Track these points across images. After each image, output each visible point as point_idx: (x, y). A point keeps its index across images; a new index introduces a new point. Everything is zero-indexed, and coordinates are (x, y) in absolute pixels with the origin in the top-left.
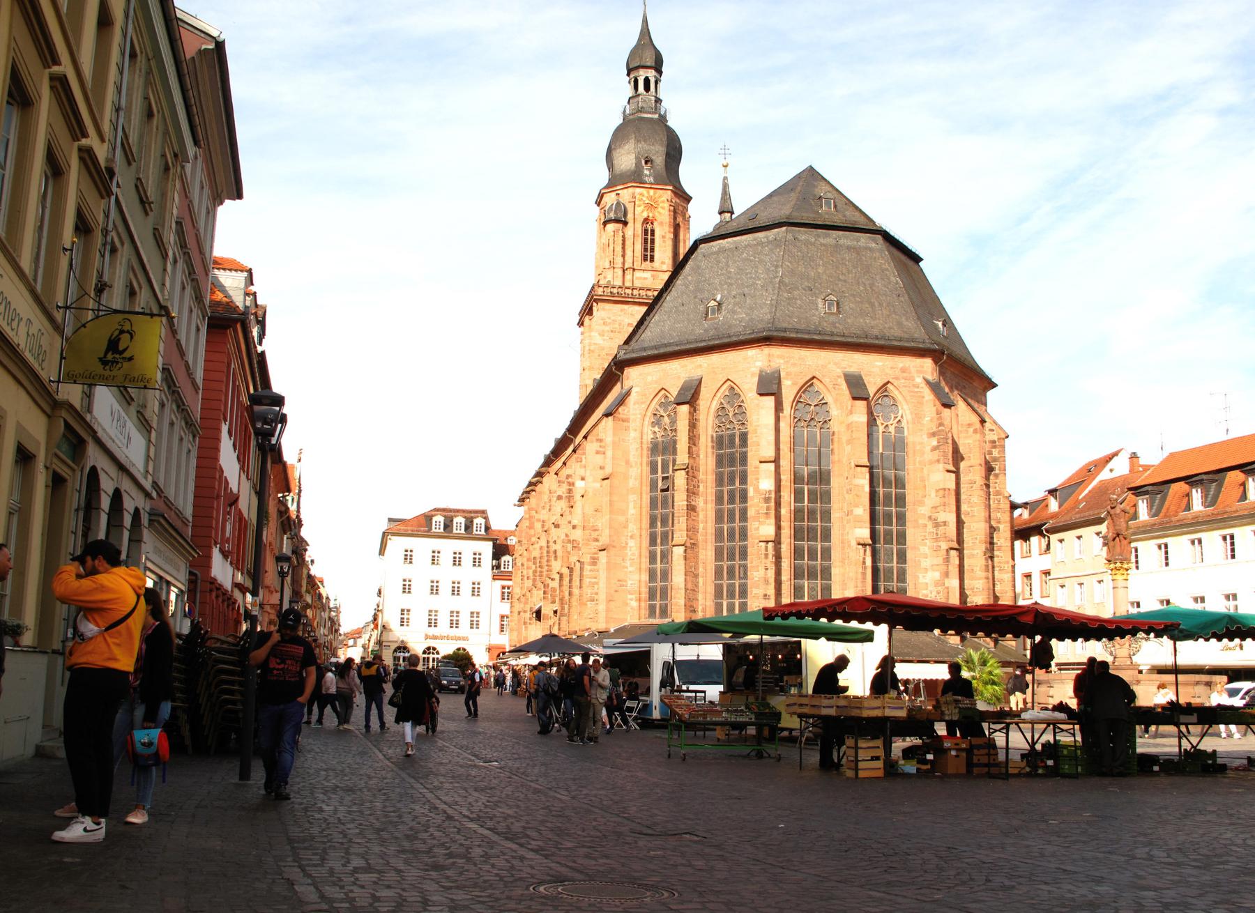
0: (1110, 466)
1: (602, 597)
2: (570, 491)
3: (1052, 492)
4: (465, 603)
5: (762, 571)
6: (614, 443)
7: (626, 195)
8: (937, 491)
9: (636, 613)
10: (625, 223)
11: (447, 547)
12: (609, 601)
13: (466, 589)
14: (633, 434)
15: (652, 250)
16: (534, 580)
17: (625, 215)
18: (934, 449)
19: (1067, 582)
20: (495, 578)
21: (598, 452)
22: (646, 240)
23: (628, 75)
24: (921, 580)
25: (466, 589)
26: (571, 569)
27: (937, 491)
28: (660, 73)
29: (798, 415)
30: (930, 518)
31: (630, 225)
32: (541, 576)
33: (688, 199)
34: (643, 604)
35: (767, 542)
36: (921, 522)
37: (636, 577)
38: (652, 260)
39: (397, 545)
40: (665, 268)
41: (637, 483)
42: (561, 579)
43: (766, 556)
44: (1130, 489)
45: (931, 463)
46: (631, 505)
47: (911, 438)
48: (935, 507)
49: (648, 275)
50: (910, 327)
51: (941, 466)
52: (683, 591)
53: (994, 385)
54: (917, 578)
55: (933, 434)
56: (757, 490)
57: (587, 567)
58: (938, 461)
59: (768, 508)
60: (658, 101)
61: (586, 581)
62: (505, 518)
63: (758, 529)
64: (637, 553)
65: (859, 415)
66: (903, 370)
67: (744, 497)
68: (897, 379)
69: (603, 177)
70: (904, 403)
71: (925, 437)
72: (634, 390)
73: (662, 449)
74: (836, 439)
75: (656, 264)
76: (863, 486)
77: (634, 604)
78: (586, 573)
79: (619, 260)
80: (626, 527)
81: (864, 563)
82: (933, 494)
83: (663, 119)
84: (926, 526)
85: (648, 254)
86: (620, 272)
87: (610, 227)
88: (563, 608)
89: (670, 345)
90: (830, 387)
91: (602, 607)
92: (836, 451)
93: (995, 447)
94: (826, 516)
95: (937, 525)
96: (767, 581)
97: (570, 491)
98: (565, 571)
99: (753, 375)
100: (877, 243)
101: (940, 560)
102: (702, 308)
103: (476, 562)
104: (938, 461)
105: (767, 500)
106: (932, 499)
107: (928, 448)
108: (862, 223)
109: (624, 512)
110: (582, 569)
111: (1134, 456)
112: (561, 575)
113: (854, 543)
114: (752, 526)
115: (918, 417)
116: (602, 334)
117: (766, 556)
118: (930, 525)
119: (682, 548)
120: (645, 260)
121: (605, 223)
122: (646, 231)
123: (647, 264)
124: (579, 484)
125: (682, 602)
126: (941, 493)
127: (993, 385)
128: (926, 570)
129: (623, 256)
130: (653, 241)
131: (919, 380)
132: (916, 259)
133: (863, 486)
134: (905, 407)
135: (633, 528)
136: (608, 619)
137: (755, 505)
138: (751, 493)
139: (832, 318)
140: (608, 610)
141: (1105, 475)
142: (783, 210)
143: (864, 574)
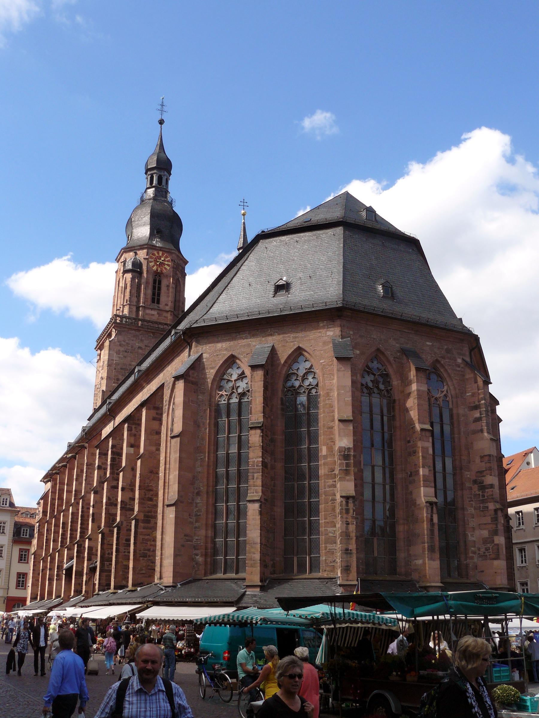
8: (482, 457)
15: (159, 295)
21: (154, 419)
22: (154, 288)
23: (146, 173)
24: (470, 538)
27: (482, 457)
28: (170, 174)
30: (475, 482)
33: (186, 262)
34: (209, 560)
36: (468, 485)
37: (203, 532)
38: (158, 302)
40: (167, 308)
48: (481, 472)
49: (155, 313)
54: (465, 535)
57: (141, 525)
59: (348, 465)
60: (167, 192)
61: (140, 537)
68: (443, 357)
70: (448, 379)
71: (466, 410)
72: (205, 356)
74: (397, 407)
75: (161, 306)
76: (427, 449)
77: (200, 559)
81: (432, 520)
82: (478, 460)
83: (171, 204)
85: (156, 298)
86: (134, 309)
87: (129, 276)
90: (391, 359)
99: (325, 343)
101: (488, 519)
105: (346, 457)
116: (118, 353)
118: (475, 488)
119: (257, 506)
120: (153, 302)
123: (155, 305)
125: (257, 556)
128: (474, 529)
130: (159, 289)
131: (459, 361)
134: (449, 383)
138: (324, 451)
142: (337, 214)
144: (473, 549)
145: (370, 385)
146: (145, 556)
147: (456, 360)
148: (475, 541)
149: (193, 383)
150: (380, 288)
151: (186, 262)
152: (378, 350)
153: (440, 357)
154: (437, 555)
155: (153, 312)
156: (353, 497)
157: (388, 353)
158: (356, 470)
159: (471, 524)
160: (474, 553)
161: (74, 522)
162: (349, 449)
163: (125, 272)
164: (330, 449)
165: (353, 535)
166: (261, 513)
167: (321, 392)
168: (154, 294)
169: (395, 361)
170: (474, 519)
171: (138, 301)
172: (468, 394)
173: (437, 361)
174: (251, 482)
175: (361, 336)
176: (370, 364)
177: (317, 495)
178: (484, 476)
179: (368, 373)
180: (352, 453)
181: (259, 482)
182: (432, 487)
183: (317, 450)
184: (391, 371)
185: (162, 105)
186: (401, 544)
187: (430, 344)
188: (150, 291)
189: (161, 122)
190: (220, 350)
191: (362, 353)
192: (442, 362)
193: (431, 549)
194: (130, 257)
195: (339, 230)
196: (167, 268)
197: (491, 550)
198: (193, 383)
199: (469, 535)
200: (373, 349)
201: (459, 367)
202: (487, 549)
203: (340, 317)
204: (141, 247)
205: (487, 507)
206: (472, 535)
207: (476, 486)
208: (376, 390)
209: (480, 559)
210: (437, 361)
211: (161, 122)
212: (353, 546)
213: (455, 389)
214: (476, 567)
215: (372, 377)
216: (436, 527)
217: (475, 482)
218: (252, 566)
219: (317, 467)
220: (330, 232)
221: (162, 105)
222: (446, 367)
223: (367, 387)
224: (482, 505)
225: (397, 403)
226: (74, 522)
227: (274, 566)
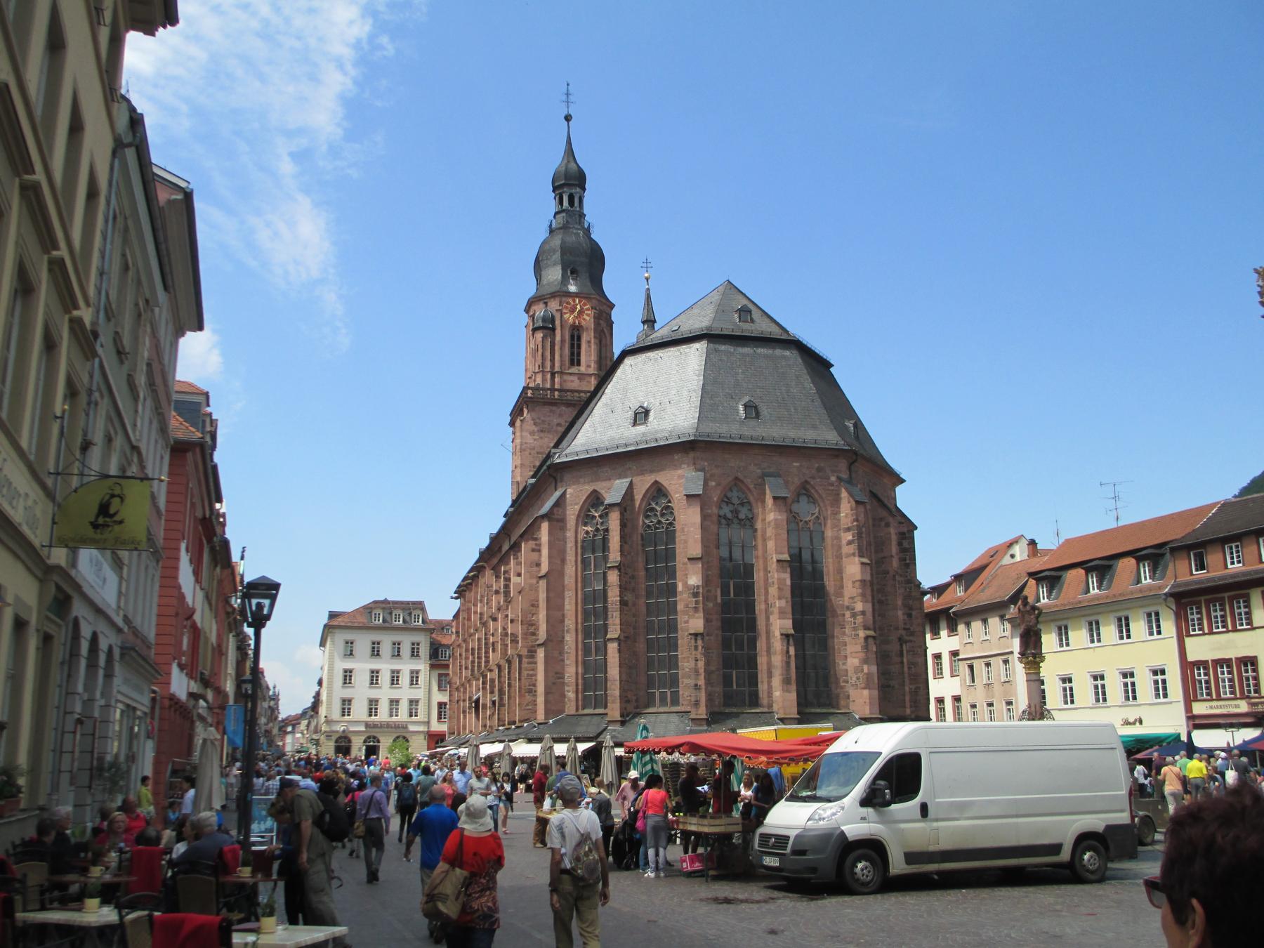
0: (1011, 552)
1: (541, 688)
2: (507, 586)
3: (957, 578)
4: (405, 693)
5: (692, 664)
6: (549, 542)
7: (554, 305)
9: (574, 704)
10: (553, 329)
11: (386, 641)
12: (547, 693)
13: (405, 679)
14: (570, 534)
15: (579, 354)
16: (473, 670)
17: (553, 320)
18: (849, 543)
19: (976, 663)
20: (433, 667)
21: (533, 550)
22: (572, 346)
24: (842, 667)
25: (405, 679)
26: (509, 662)
28: (584, 189)
29: (722, 513)
31: (558, 332)
32: (479, 666)
33: (612, 306)
35: (696, 635)
38: (579, 364)
39: (340, 638)
40: (591, 371)
41: (573, 580)
42: (500, 671)
43: (696, 648)
44: (1031, 575)
45: (848, 556)
46: (567, 602)
48: (852, 598)
51: (857, 559)
52: (618, 683)
53: (903, 481)
55: (848, 529)
56: (685, 584)
57: (525, 660)
58: (854, 554)
59: (697, 603)
60: (582, 215)
61: (525, 673)
62: (442, 608)
63: (687, 622)
64: (573, 647)
66: (819, 470)
67: (671, 590)
68: (813, 478)
69: (531, 289)
73: (595, 546)
75: (583, 369)
77: (571, 695)
78: (524, 665)
79: (548, 364)
80: (563, 621)
81: (788, 652)
82: (850, 585)
83: (587, 232)
85: (575, 360)
86: (549, 376)
87: (539, 335)
88: (501, 699)
89: (602, 449)
90: (751, 486)
91: (541, 700)
92: (760, 547)
93: (905, 538)
94: (750, 607)
95: (854, 615)
96: (696, 671)
97: (507, 586)
98: (503, 663)
101: (859, 648)
102: (631, 414)
103: (415, 653)
104: (854, 554)
105: (695, 595)
107: (844, 542)
108: (776, 332)
109: (561, 608)
110: (520, 663)
111: (1032, 543)
112: (499, 667)
113: (777, 634)
114: (681, 619)
116: (532, 433)
117: (696, 648)
118: (848, 614)
121: (535, 330)
122: (572, 337)
123: (574, 370)
124: (514, 579)
125: (617, 693)
126: (858, 584)
127: (903, 481)
129: (553, 360)
130: (579, 347)
131: (833, 479)
132: (829, 365)
135: (570, 622)
136: (548, 713)
137: (683, 600)
138: (680, 587)
139: (753, 423)
140: (546, 702)
141: (1007, 560)
143: (788, 663)
145: (729, 515)
146: (530, 691)
149: (558, 521)
150: (741, 408)
151: (612, 306)
152: (737, 478)
154: (794, 687)
155: (571, 378)
156: (702, 634)
157: (748, 481)
158: (711, 605)
159: (843, 653)
161: (479, 649)
163: (535, 330)
164: (685, 584)
165: (702, 671)
166: (620, 651)
167: (678, 527)
168: (572, 354)
171: (553, 366)
173: (806, 482)
174: (610, 621)
175: (717, 466)
176: (729, 495)
177: (676, 631)
179: (727, 503)
181: (618, 621)
183: (675, 585)
184: (751, 498)
185: (568, 94)
186: (762, 676)
188: (567, 351)
189: (568, 118)
191: (718, 484)
193: (786, 681)
194: (539, 310)
195: (701, 346)
196: (588, 319)
198: (558, 521)
200: (730, 479)
204: (553, 295)
208: (735, 521)
210: (806, 482)
211: (568, 118)
212: (702, 682)
214: (848, 697)
215: (731, 507)
216: (793, 659)
217: (848, 608)
218: (613, 702)
219: (675, 603)
220: (696, 345)
221: (568, 94)
223: (725, 517)
226: (479, 649)
227: (637, 701)
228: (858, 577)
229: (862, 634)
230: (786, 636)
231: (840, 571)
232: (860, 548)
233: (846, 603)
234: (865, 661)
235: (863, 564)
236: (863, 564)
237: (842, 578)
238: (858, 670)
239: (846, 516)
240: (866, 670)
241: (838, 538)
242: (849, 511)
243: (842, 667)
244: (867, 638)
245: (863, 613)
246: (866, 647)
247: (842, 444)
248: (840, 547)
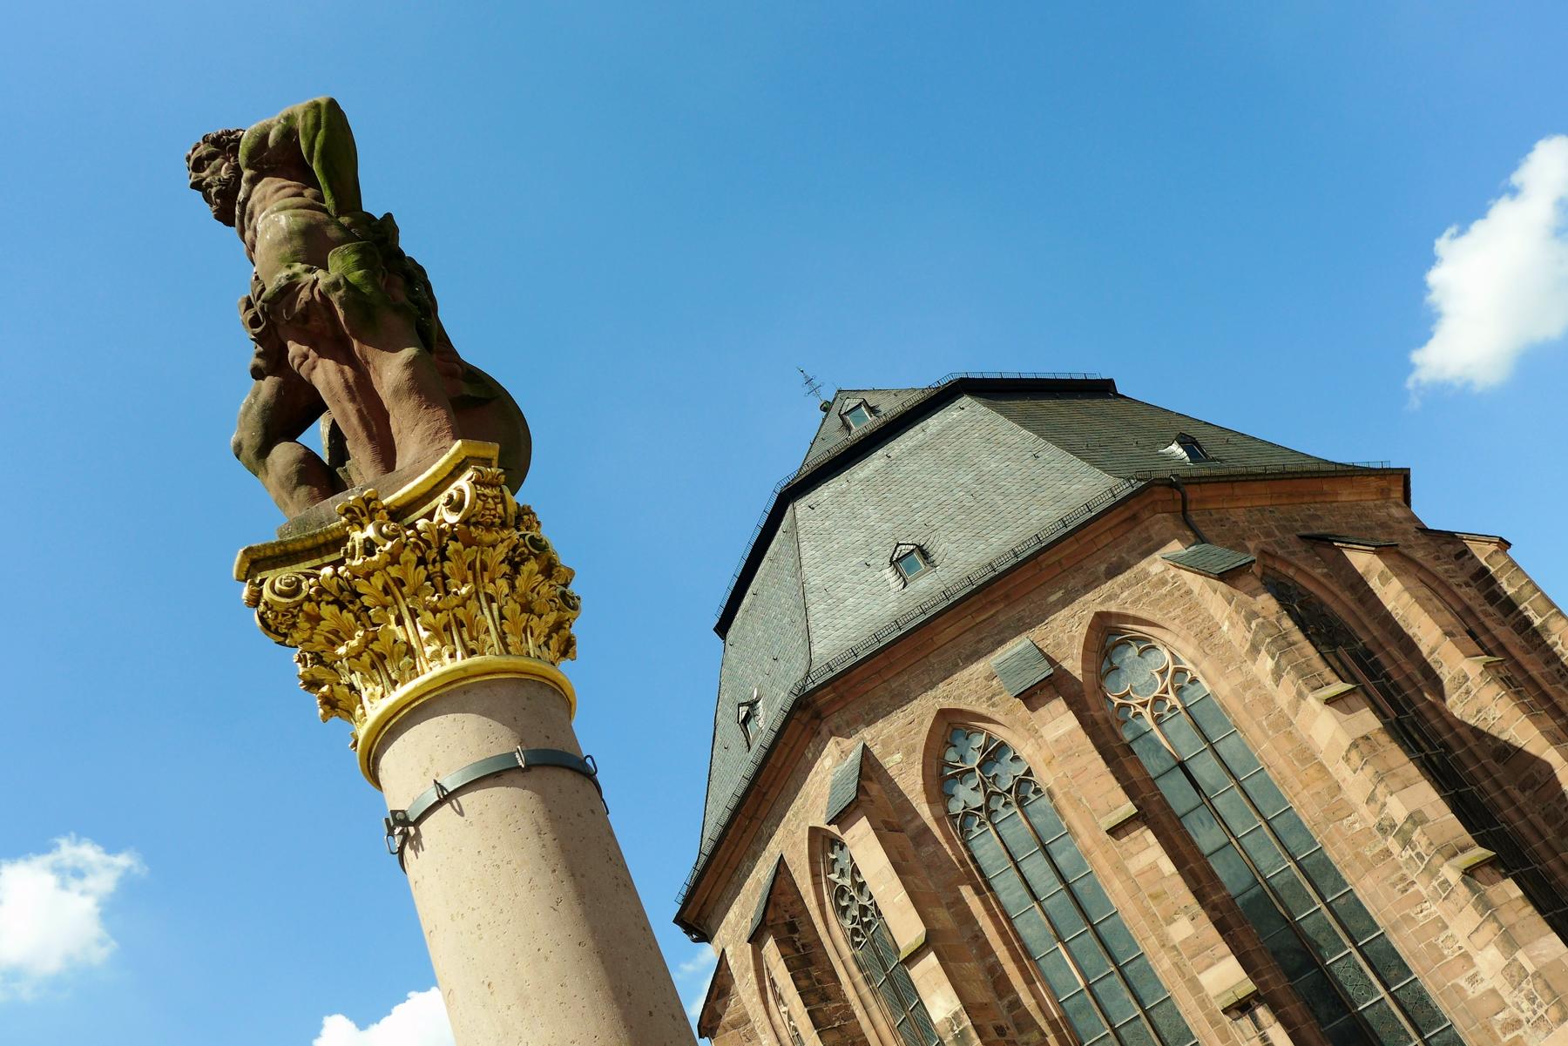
18: (1277, 675)
24: (1473, 992)
27: (1347, 759)
30: (1382, 829)
47: (1216, 683)
48: (1371, 799)
50: (1078, 486)
55: (1255, 649)
58: (1301, 695)
65: (1059, 721)
76: (1154, 867)
84: (1387, 853)
100: (966, 409)
104: (1301, 695)
106: (1355, 782)
107: (1268, 681)
115: (1207, 636)
118: (1393, 844)
126: (1354, 755)
128: (1466, 957)
132: (1104, 388)
133: (1154, 867)
134: (1167, 638)
144: (1501, 1016)
147: (1148, 574)
148: (1494, 991)
153: (1101, 603)
160: (1517, 1024)
162: (956, 1016)
169: (993, 705)
170: (1449, 932)
172: (1225, 628)
178: (1384, 805)
180: (967, 1023)
182: (1223, 957)
187: (1060, 594)
190: (737, 924)
191: (909, 752)
192: (1114, 610)
197: (1539, 999)
199: (1463, 983)
201: (1164, 582)
202: (1532, 1000)
203: (818, 716)
205: (1446, 881)
206: (1473, 980)
207: (1390, 838)
209: (1541, 1034)
213: (1185, 640)
222: (1131, 612)
224: (1435, 883)
225: (1056, 790)
228: (1346, 743)
229: (1451, 873)
230: (1242, 1007)
231: (1306, 755)
232: (1304, 672)
233: (1373, 821)
234: (1509, 941)
235: (1329, 702)
236: (1329, 702)
237: (1322, 768)
238: (1515, 975)
239: (1233, 625)
240: (1530, 968)
241: (1251, 683)
242: (1229, 609)
243: (1473, 992)
244: (1469, 873)
245: (1416, 819)
246: (1486, 906)
247: (1124, 490)
248: (1269, 701)
